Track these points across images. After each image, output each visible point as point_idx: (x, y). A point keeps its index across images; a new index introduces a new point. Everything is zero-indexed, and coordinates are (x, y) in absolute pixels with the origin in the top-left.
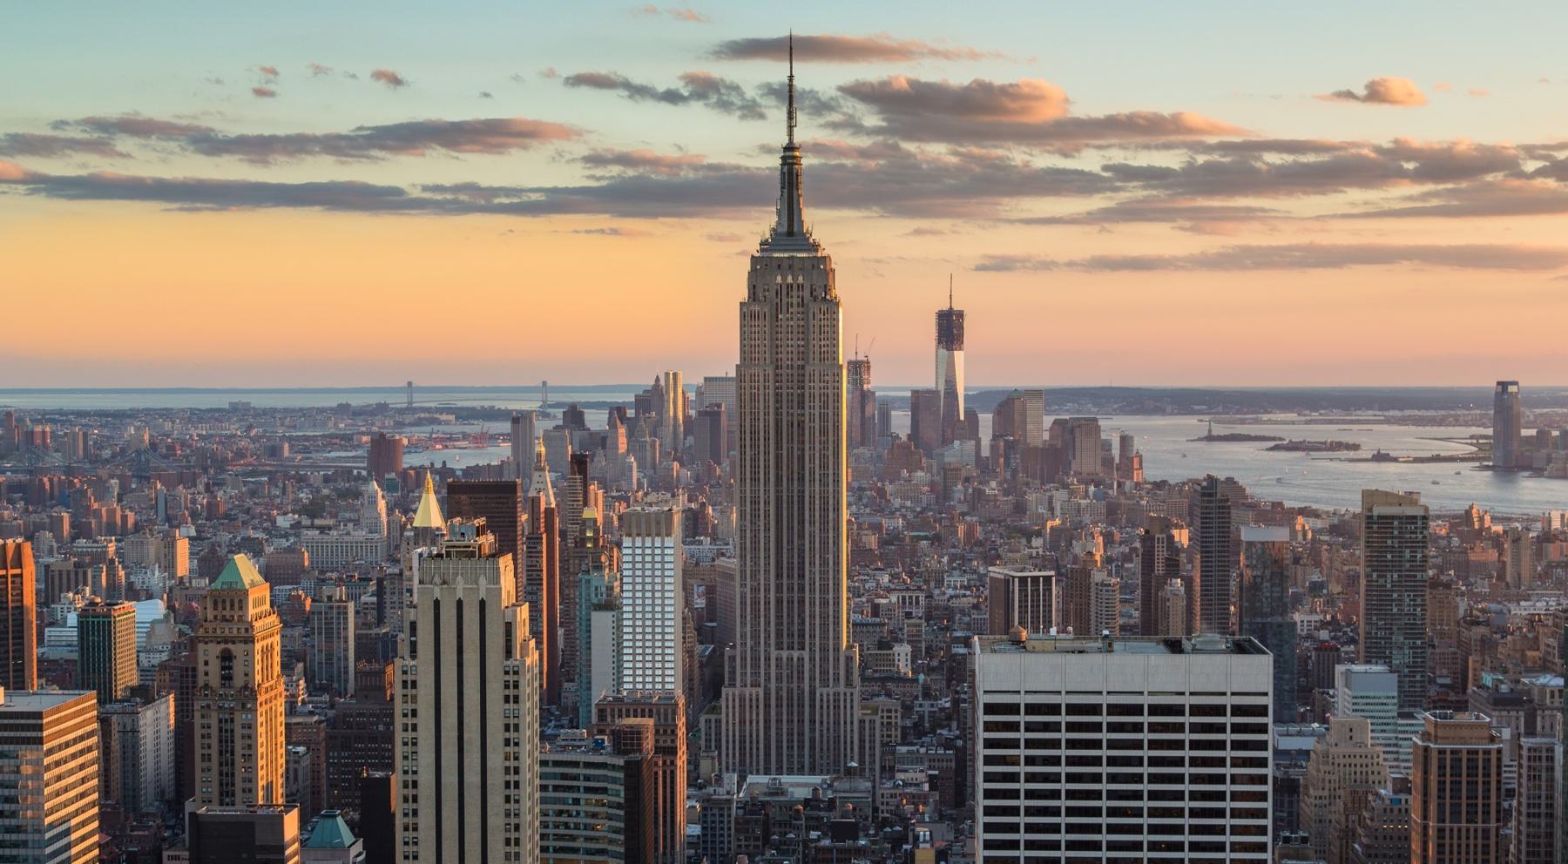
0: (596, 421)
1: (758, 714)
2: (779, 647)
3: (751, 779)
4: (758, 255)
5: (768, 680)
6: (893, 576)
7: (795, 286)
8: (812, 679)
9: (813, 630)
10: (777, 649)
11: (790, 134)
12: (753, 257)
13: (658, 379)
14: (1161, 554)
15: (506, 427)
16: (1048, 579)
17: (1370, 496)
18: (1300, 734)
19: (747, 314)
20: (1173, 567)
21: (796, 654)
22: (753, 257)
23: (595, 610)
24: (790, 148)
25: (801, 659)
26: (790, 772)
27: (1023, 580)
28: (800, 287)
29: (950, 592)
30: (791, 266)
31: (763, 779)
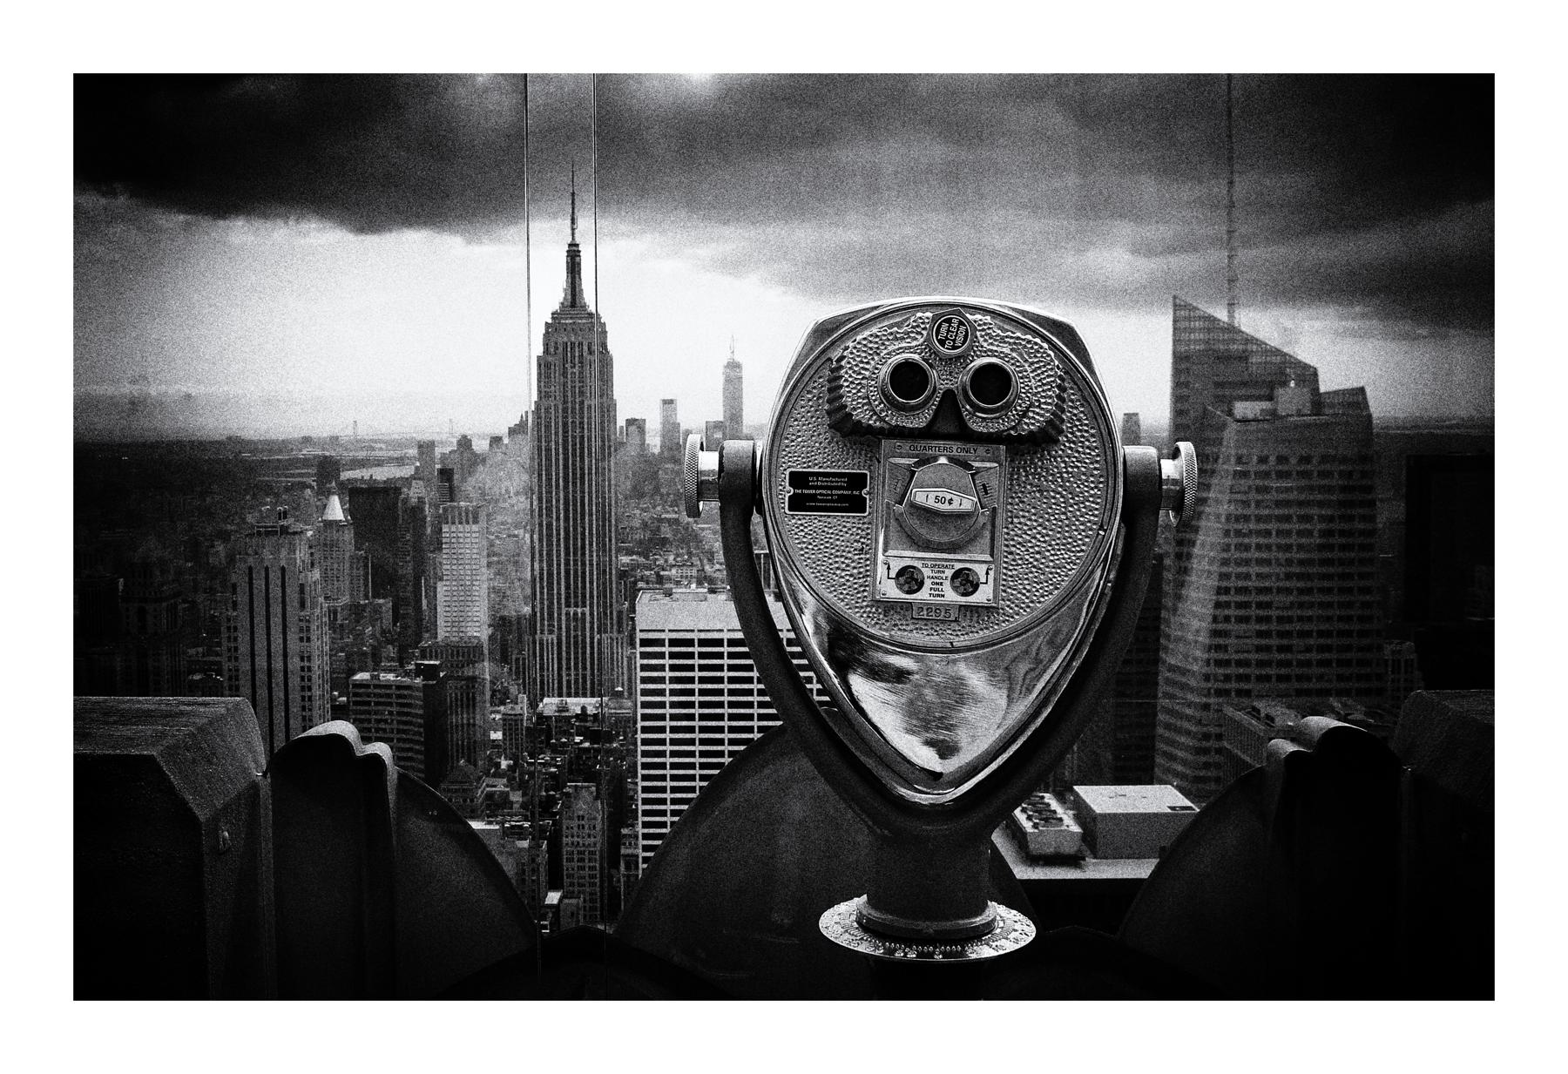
0: (481, 446)
1: (553, 654)
2: (568, 605)
3: (546, 700)
4: (550, 321)
5: (560, 628)
6: (677, 555)
7: (577, 344)
8: (592, 628)
9: (591, 592)
10: (566, 607)
11: (573, 234)
12: (546, 323)
13: (522, 417)
15: (413, 452)
19: (544, 366)
21: (579, 610)
22: (546, 323)
25: (583, 614)
26: (577, 695)
31: (556, 700)
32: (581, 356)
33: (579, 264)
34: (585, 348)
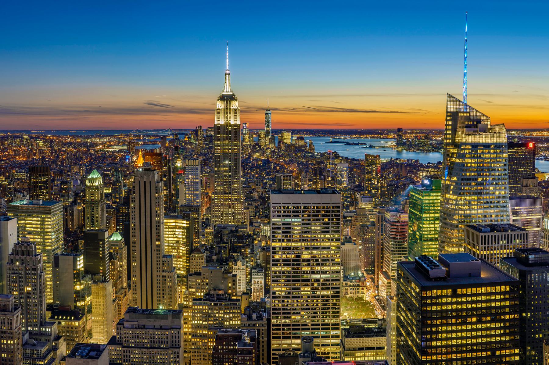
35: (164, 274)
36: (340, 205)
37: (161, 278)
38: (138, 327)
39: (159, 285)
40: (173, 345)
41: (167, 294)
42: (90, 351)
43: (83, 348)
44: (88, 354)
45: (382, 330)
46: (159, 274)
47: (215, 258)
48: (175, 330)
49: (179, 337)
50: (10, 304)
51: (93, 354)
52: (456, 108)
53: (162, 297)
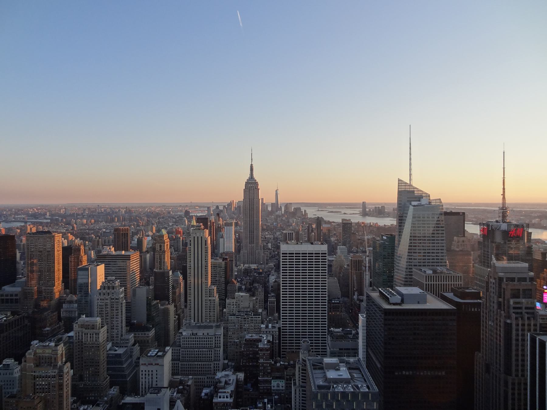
2: (250, 244)
3: (245, 265)
5: (248, 249)
6: (268, 233)
14: (310, 229)
16: (293, 233)
17: (343, 220)
18: (332, 257)
19: (245, 191)
20: (312, 231)
23: (221, 238)
24: (252, 165)
25: (253, 246)
27: (289, 233)
28: (253, 187)
29: (277, 235)
30: (252, 183)
31: (247, 265)
32: (253, 189)
33: (253, 169)
34: (254, 187)
35: (210, 298)
36: (327, 252)
37: (208, 301)
38: (192, 334)
39: (206, 306)
40: (216, 346)
41: (212, 312)
42: (158, 352)
43: (153, 350)
44: (156, 354)
45: (355, 337)
46: (206, 298)
47: (243, 287)
48: (218, 336)
49: (220, 341)
50: (98, 324)
51: (160, 354)
52: (405, 188)
53: (208, 314)
